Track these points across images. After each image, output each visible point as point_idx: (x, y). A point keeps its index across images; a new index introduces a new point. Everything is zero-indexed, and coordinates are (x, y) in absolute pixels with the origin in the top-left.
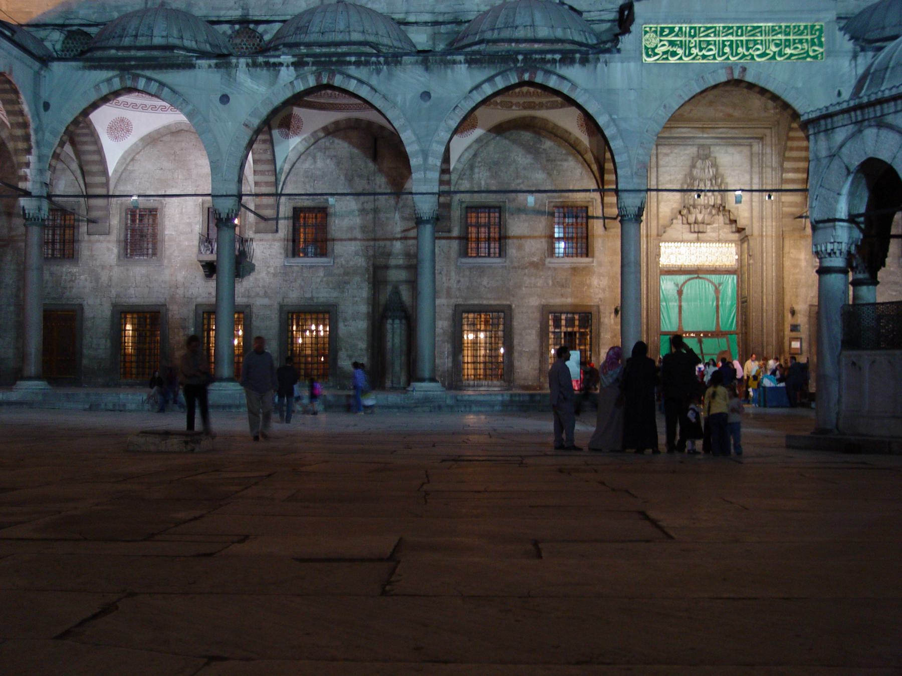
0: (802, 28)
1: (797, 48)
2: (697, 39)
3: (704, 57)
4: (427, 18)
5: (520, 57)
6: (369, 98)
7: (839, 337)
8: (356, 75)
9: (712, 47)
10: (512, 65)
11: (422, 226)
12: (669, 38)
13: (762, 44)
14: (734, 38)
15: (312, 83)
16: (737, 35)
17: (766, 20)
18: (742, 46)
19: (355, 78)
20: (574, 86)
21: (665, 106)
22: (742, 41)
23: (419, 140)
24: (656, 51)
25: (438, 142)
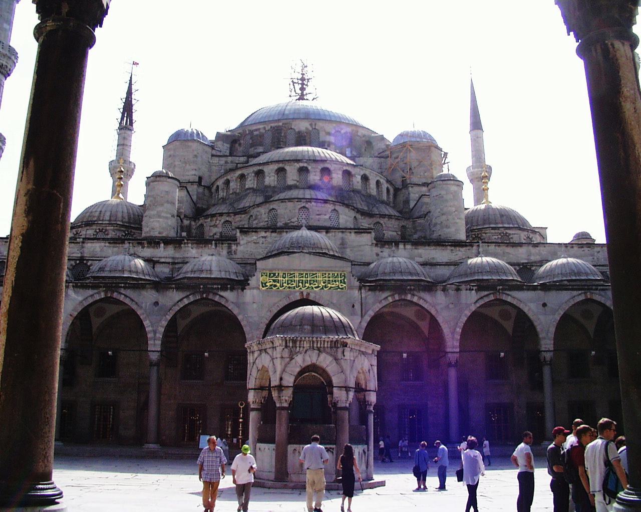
0: (336, 275)
1: (334, 284)
2: (286, 279)
3: (289, 287)
4: (170, 260)
5: (202, 286)
7: (257, 437)
8: (124, 293)
9: (294, 283)
10: (198, 290)
11: (152, 367)
12: (273, 278)
13: (317, 282)
14: (304, 279)
15: (103, 295)
16: (305, 278)
17: (319, 271)
18: (308, 283)
19: (123, 294)
20: (227, 301)
21: (270, 311)
22: (307, 280)
23: (152, 326)
24: (267, 284)
25: (161, 326)
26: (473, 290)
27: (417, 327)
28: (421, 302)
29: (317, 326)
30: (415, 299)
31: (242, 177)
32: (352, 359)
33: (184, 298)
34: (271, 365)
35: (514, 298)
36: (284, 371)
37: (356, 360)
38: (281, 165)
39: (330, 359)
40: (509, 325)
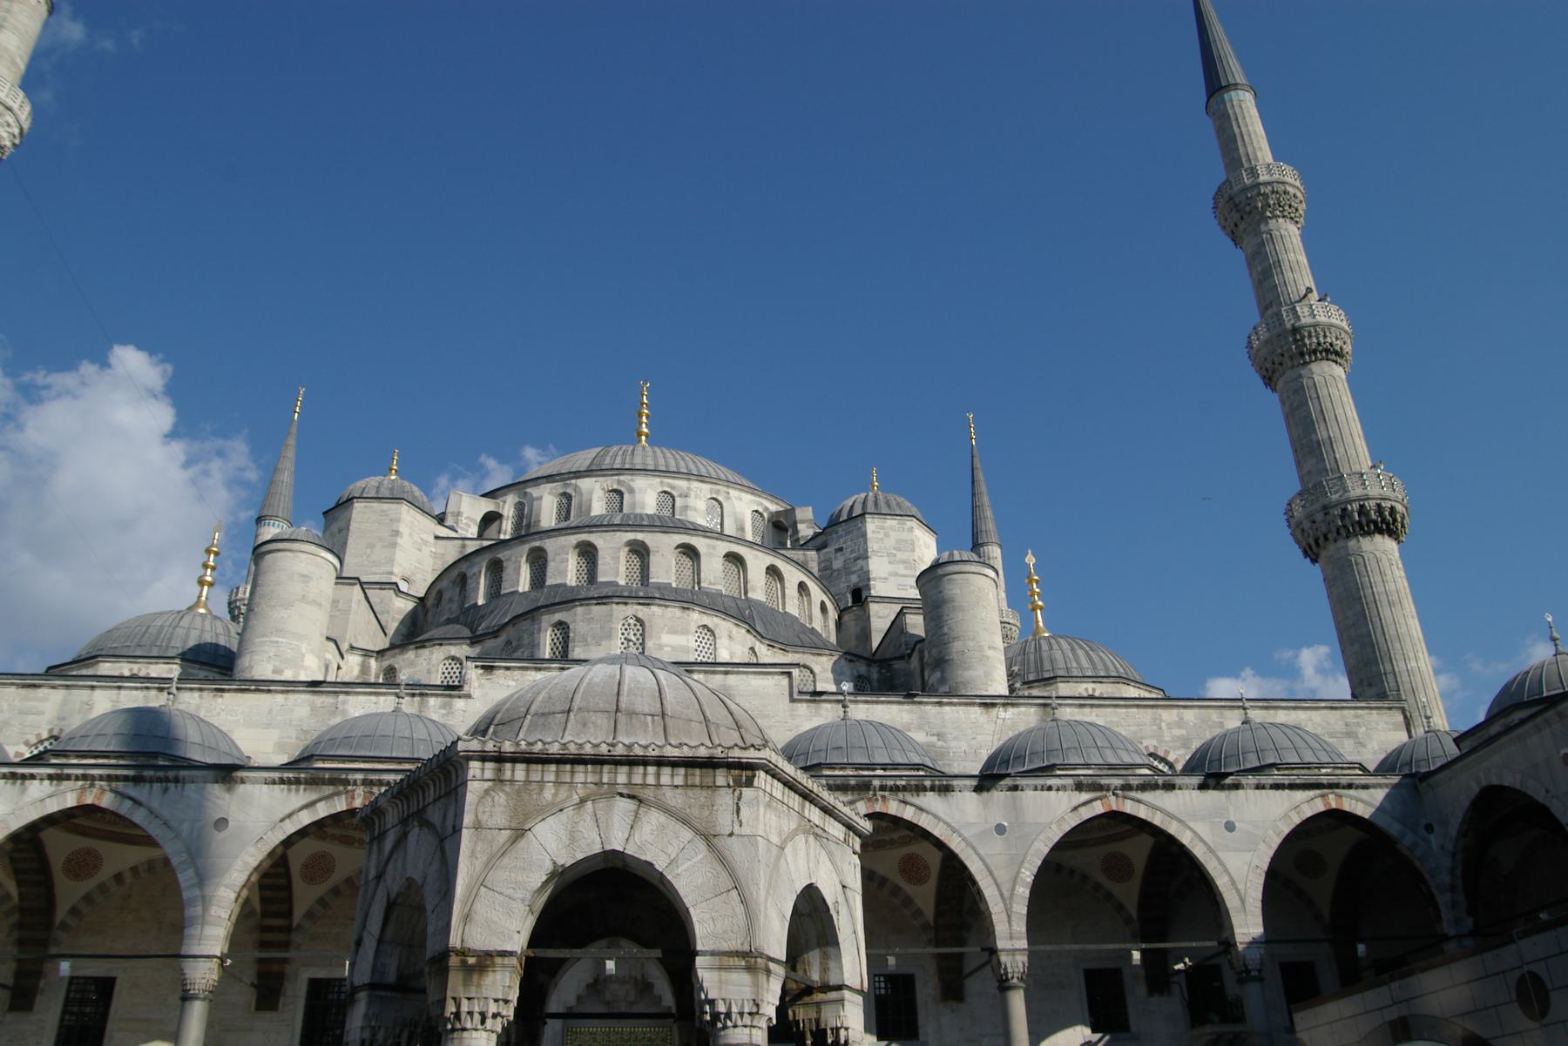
6: (144, 825)
15: (70, 801)
26: (1050, 788)
27: (908, 901)
28: (924, 822)
29: (632, 714)
30: (908, 814)
31: (496, 568)
32: (775, 839)
33: (301, 809)
34: (435, 866)
35: (1155, 808)
36: (481, 882)
37: (788, 850)
38: (584, 537)
39: (687, 834)
40: (1128, 893)
